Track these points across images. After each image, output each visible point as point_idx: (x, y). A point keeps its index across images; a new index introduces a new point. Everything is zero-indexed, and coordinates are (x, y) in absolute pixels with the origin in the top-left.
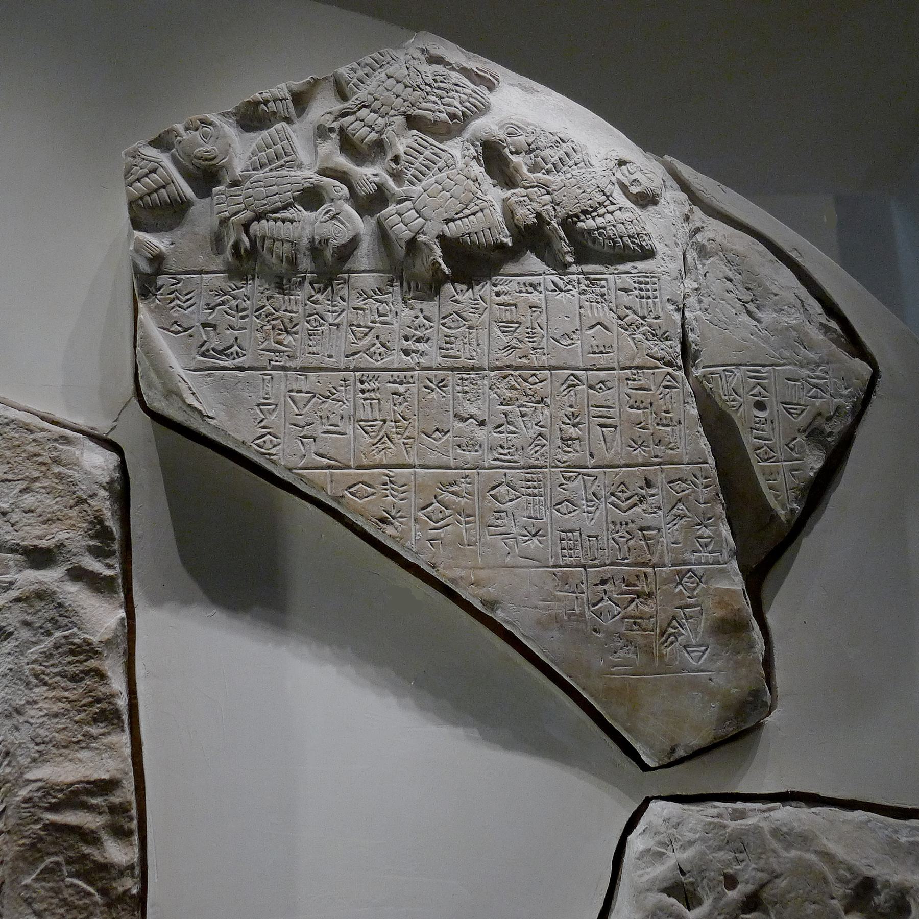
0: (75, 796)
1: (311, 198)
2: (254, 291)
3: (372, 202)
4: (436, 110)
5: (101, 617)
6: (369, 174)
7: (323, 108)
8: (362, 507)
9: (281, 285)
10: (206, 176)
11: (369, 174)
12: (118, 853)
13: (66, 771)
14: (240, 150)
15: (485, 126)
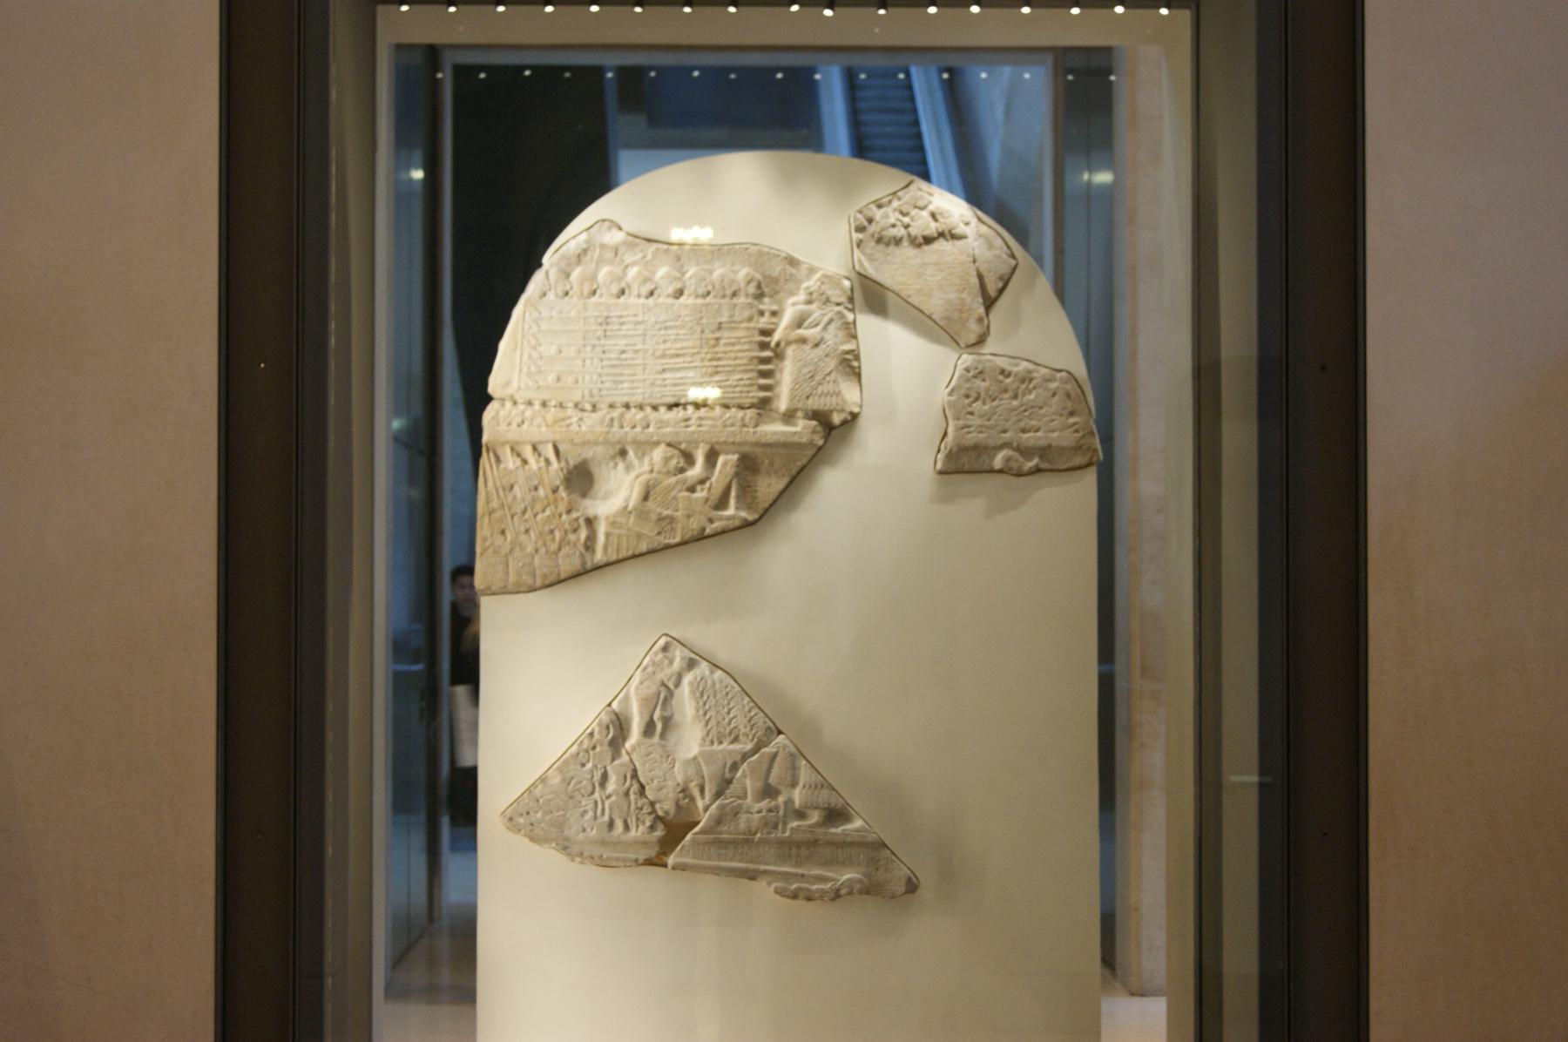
0: (848, 352)
1: (894, 226)
2: (881, 246)
3: (907, 227)
4: (921, 203)
5: (850, 317)
6: (906, 220)
7: (895, 204)
8: (904, 293)
9: (887, 245)
10: (870, 221)
11: (906, 220)
12: (855, 364)
13: (847, 347)
14: (878, 214)
15: (931, 208)
